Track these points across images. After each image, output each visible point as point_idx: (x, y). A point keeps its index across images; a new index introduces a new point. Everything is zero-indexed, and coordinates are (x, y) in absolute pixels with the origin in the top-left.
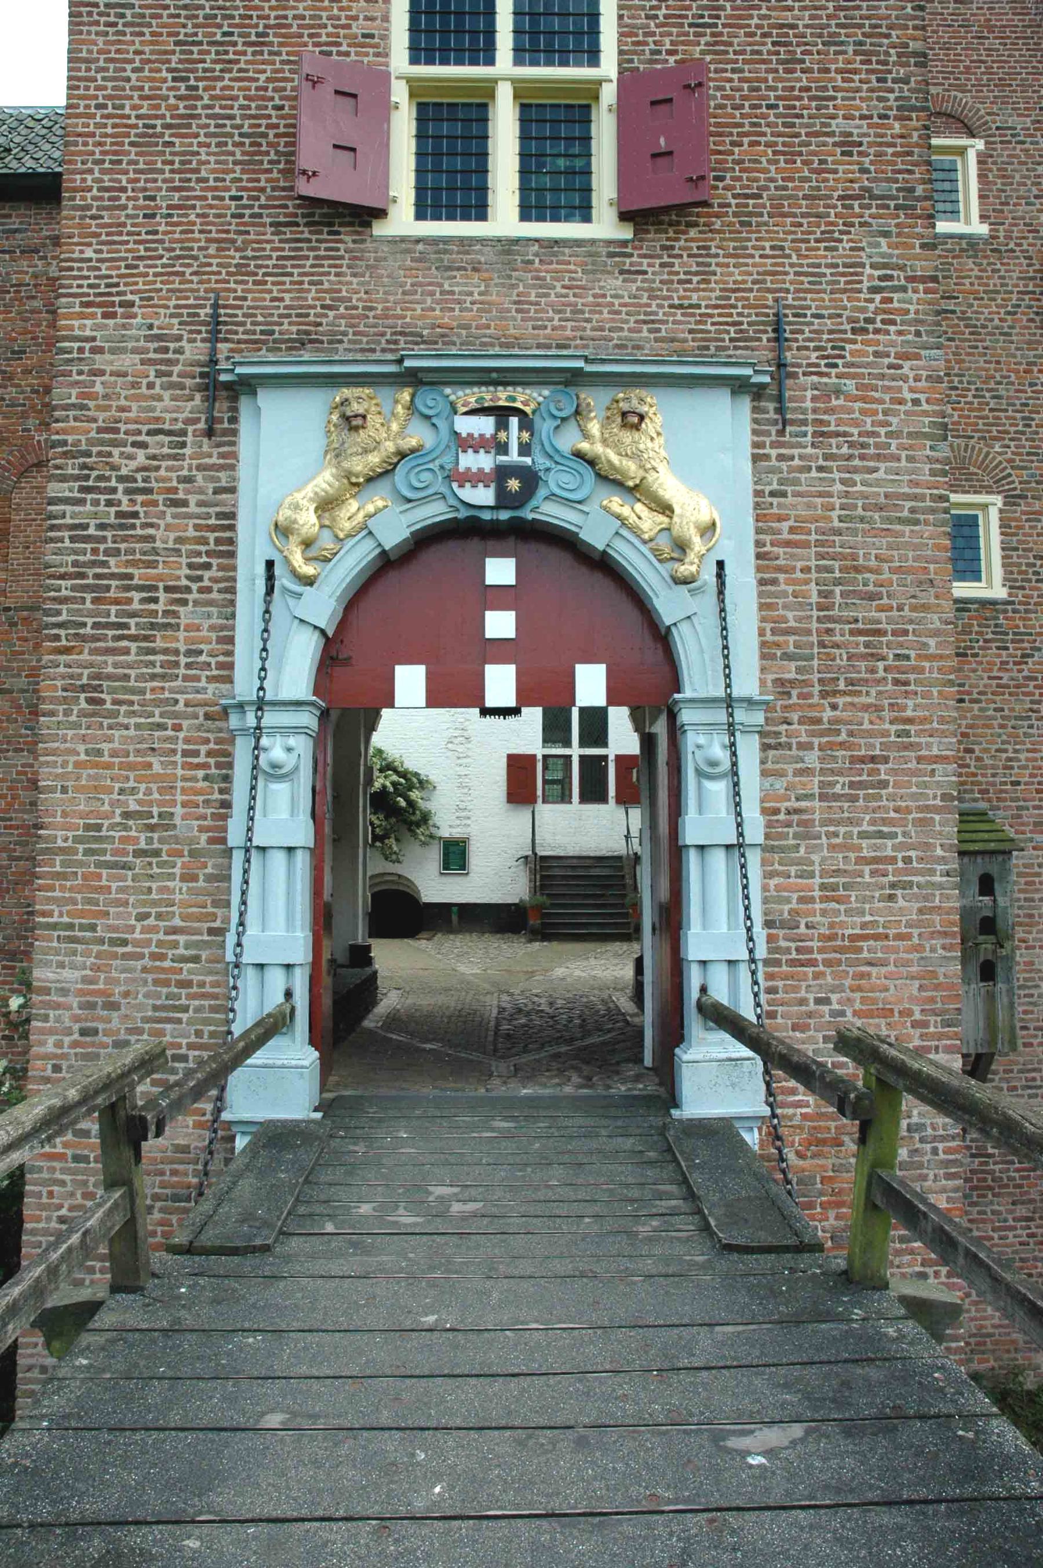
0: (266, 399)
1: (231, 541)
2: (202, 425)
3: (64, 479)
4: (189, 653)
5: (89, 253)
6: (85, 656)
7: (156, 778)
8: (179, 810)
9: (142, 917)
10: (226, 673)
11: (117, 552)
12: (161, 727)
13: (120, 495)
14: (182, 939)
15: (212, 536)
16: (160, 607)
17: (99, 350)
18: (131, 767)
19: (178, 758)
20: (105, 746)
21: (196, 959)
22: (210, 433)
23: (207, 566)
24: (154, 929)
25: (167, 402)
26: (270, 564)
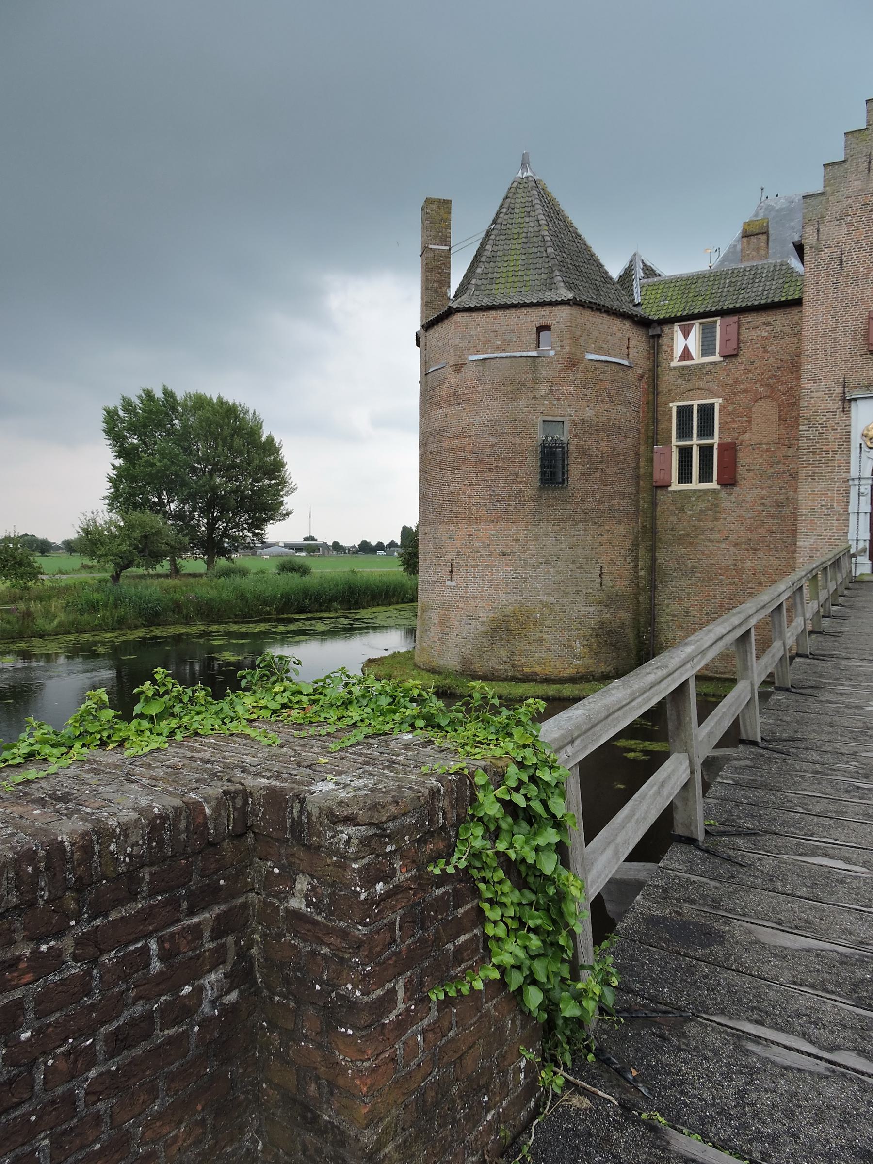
0: (858, 401)
1: (849, 438)
2: (841, 409)
3: (803, 425)
4: (838, 466)
5: (809, 367)
6: (811, 468)
7: (829, 497)
8: (835, 504)
9: (825, 530)
10: (848, 470)
11: (818, 443)
12: (831, 484)
13: (819, 428)
14: (836, 535)
15: (844, 437)
16: (830, 455)
17: (811, 392)
18: (823, 494)
19: (835, 492)
20: (816, 490)
21: (839, 539)
22: (843, 411)
23: (843, 445)
24: (829, 533)
25: (831, 404)
26: (861, 444)
